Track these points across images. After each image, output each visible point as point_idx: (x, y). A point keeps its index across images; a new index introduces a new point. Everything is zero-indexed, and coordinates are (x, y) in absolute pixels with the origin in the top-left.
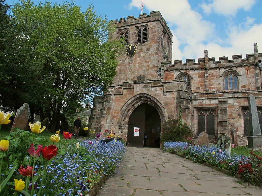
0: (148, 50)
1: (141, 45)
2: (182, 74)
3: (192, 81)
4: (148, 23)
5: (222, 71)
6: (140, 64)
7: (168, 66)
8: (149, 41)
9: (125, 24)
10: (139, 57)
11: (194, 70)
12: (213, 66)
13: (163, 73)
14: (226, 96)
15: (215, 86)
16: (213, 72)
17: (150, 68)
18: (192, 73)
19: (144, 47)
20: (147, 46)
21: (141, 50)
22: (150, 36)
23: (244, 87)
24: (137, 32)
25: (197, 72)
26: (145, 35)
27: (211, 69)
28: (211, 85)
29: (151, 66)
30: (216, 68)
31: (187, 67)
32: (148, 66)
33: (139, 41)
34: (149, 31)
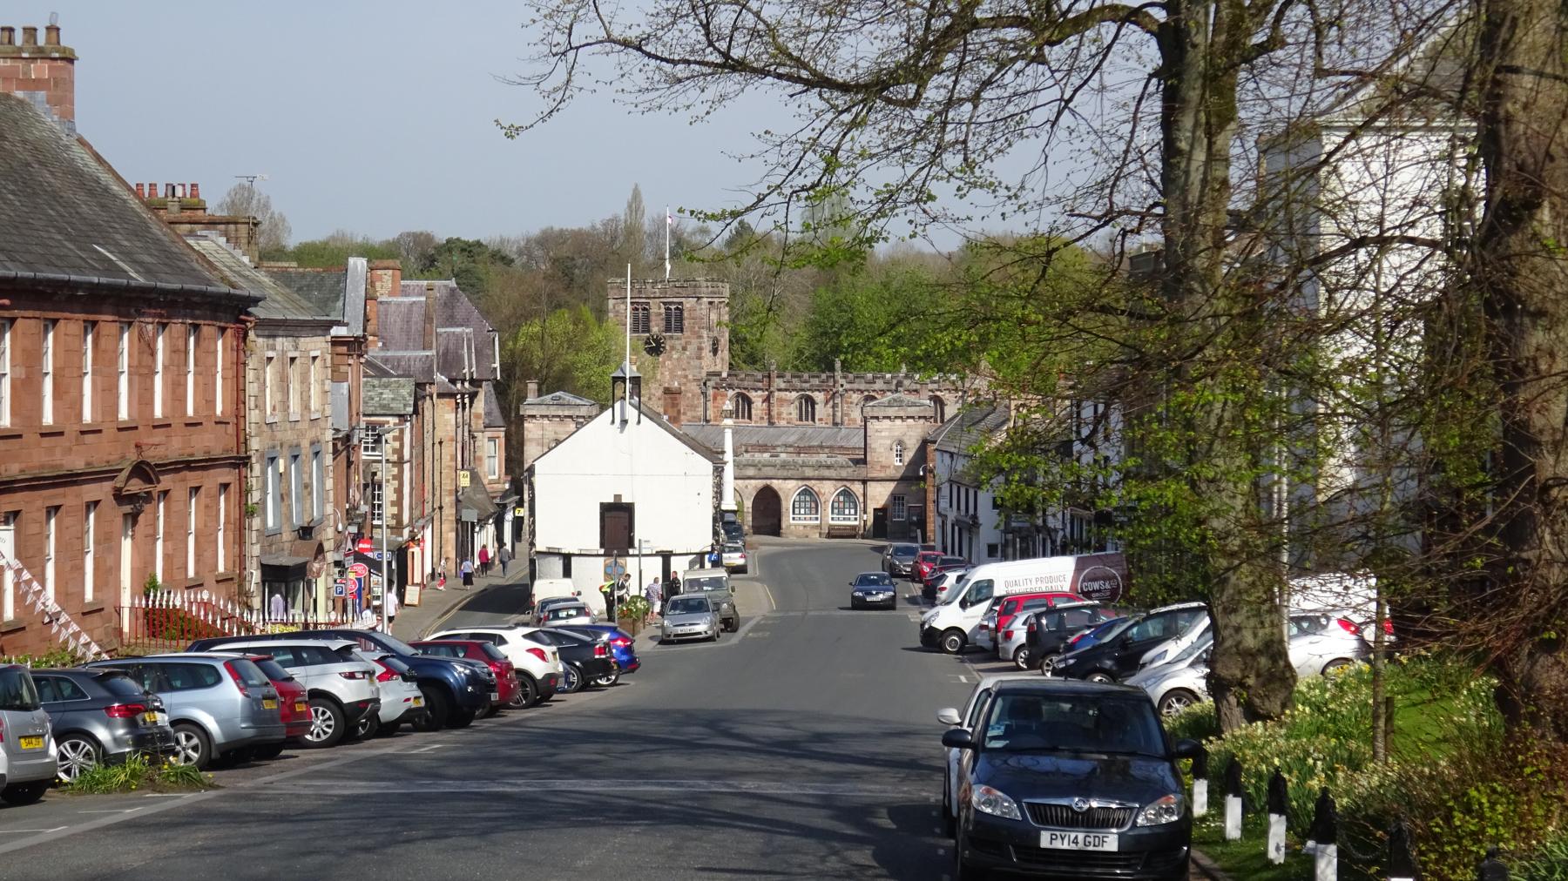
0: (684, 349)
1: (671, 337)
2: (739, 395)
3: (753, 406)
4: (683, 300)
5: (794, 395)
6: (672, 372)
7: (717, 379)
8: (686, 334)
9: (640, 292)
10: (670, 358)
11: (756, 390)
12: (783, 386)
13: (711, 392)
14: (779, 449)
15: (784, 415)
16: (783, 394)
17: (689, 381)
18: (752, 395)
19: (677, 342)
20: (683, 341)
21: (673, 348)
22: (686, 323)
23: (821, 420)
24: (663, 311)
25: (760, 393)
26: (680, 318)
27: (779, 390)
28: (779, 414)
29: (690, 377)
30: (786, 390)
31: (746, 384)
32: (686, 377)
33: (668, 329)
34: (686, 314)
